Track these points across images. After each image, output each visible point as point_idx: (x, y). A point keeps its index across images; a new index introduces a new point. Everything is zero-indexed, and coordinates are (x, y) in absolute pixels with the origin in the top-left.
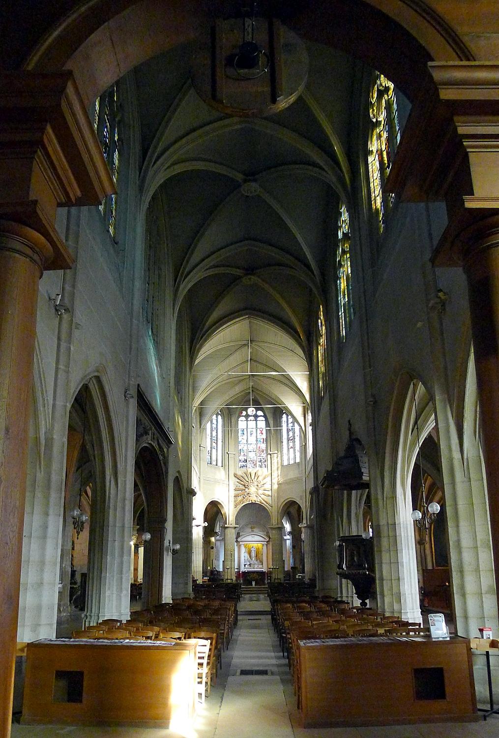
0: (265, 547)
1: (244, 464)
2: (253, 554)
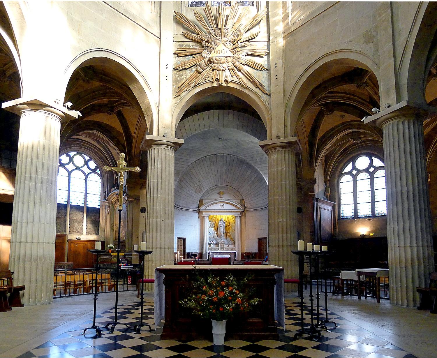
0: (238, 220)
2: (222, 230)
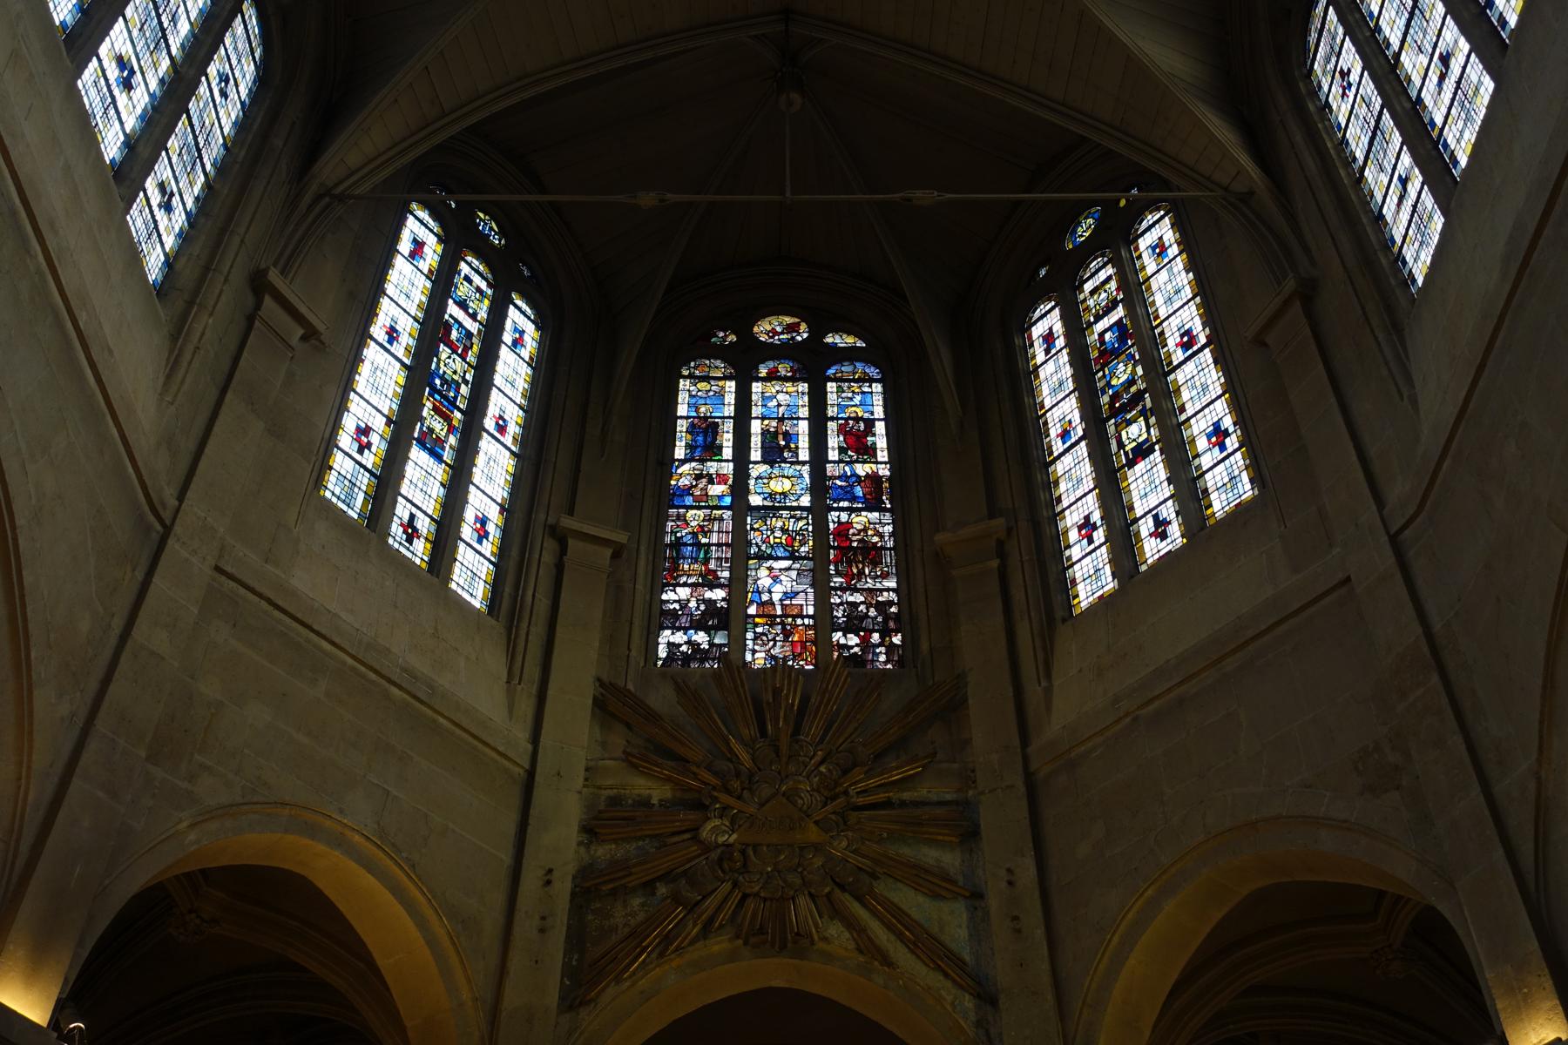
1: (701, 637)
